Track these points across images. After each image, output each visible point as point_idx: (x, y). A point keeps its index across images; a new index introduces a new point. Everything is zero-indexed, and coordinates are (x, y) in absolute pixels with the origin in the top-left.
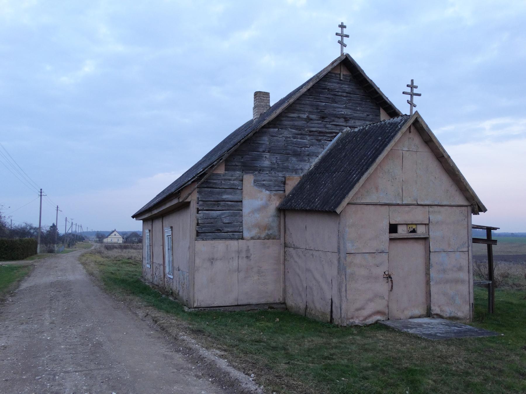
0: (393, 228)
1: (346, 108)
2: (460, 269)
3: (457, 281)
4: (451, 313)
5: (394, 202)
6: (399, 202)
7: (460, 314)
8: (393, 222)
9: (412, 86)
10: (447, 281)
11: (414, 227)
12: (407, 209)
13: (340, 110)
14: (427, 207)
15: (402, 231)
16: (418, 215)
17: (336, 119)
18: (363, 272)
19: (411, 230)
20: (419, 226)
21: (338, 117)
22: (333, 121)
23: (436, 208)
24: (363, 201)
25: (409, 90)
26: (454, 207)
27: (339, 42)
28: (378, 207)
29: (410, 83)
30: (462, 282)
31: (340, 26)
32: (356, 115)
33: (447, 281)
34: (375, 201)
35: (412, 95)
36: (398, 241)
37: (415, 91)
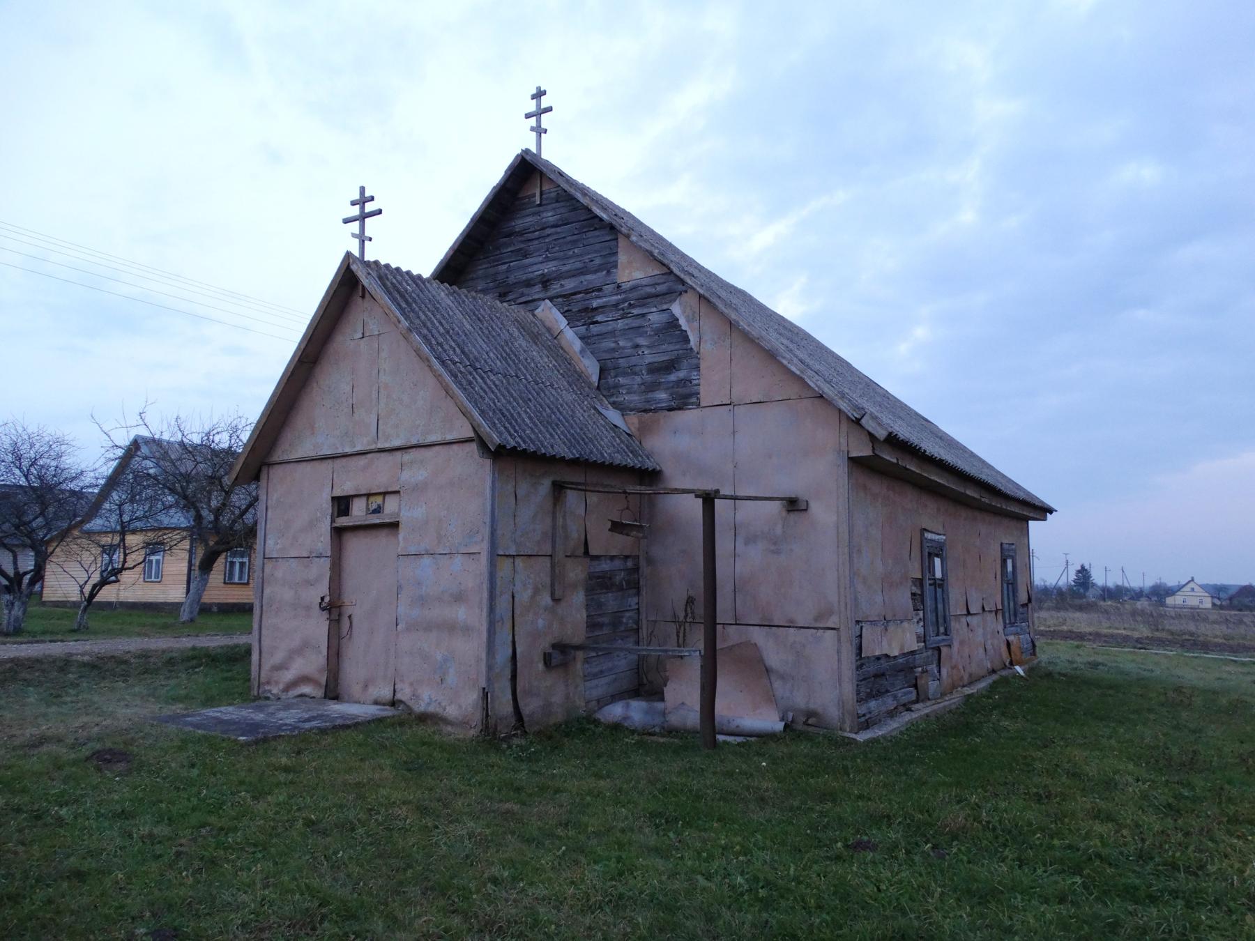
0: (342, 505)
1: (548, 260)
2: (459, 598)
3: (451, 628)
4: (429, 704)
5: (340, 451)
6: (348, 450)
7: (451, 711)
8: (338, 492)
9: (363, 200)
10: (429, 627)
11: (379, 500)
12: (362, 461)
13: (535, 268)
14: (398, 454)
15: (358, 510)
16: (379, 474)
17: (526, 290)
18: (288, 595)
19: (375, 506)
20: (389, 499)
21: (529, 284)
22: (522, 295)
23: (413, 454)
24: (293, 456)
25: (356, 211)
26: (455, 447)
27: (532, 129)
28: (316, 464)
29: (367, 194)
30: (467, 630)
31: (533, 97)
32: (564, 268)
33: (429, 627)
34: (311, 454)
35: (363, 217)
36: (361, 534)
37: (369, 207)
